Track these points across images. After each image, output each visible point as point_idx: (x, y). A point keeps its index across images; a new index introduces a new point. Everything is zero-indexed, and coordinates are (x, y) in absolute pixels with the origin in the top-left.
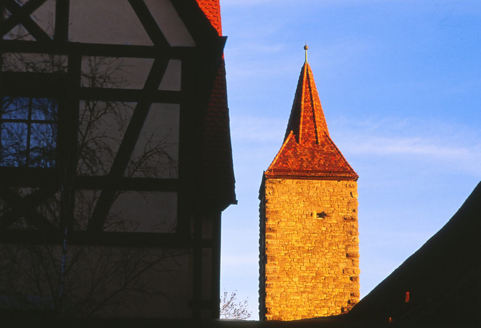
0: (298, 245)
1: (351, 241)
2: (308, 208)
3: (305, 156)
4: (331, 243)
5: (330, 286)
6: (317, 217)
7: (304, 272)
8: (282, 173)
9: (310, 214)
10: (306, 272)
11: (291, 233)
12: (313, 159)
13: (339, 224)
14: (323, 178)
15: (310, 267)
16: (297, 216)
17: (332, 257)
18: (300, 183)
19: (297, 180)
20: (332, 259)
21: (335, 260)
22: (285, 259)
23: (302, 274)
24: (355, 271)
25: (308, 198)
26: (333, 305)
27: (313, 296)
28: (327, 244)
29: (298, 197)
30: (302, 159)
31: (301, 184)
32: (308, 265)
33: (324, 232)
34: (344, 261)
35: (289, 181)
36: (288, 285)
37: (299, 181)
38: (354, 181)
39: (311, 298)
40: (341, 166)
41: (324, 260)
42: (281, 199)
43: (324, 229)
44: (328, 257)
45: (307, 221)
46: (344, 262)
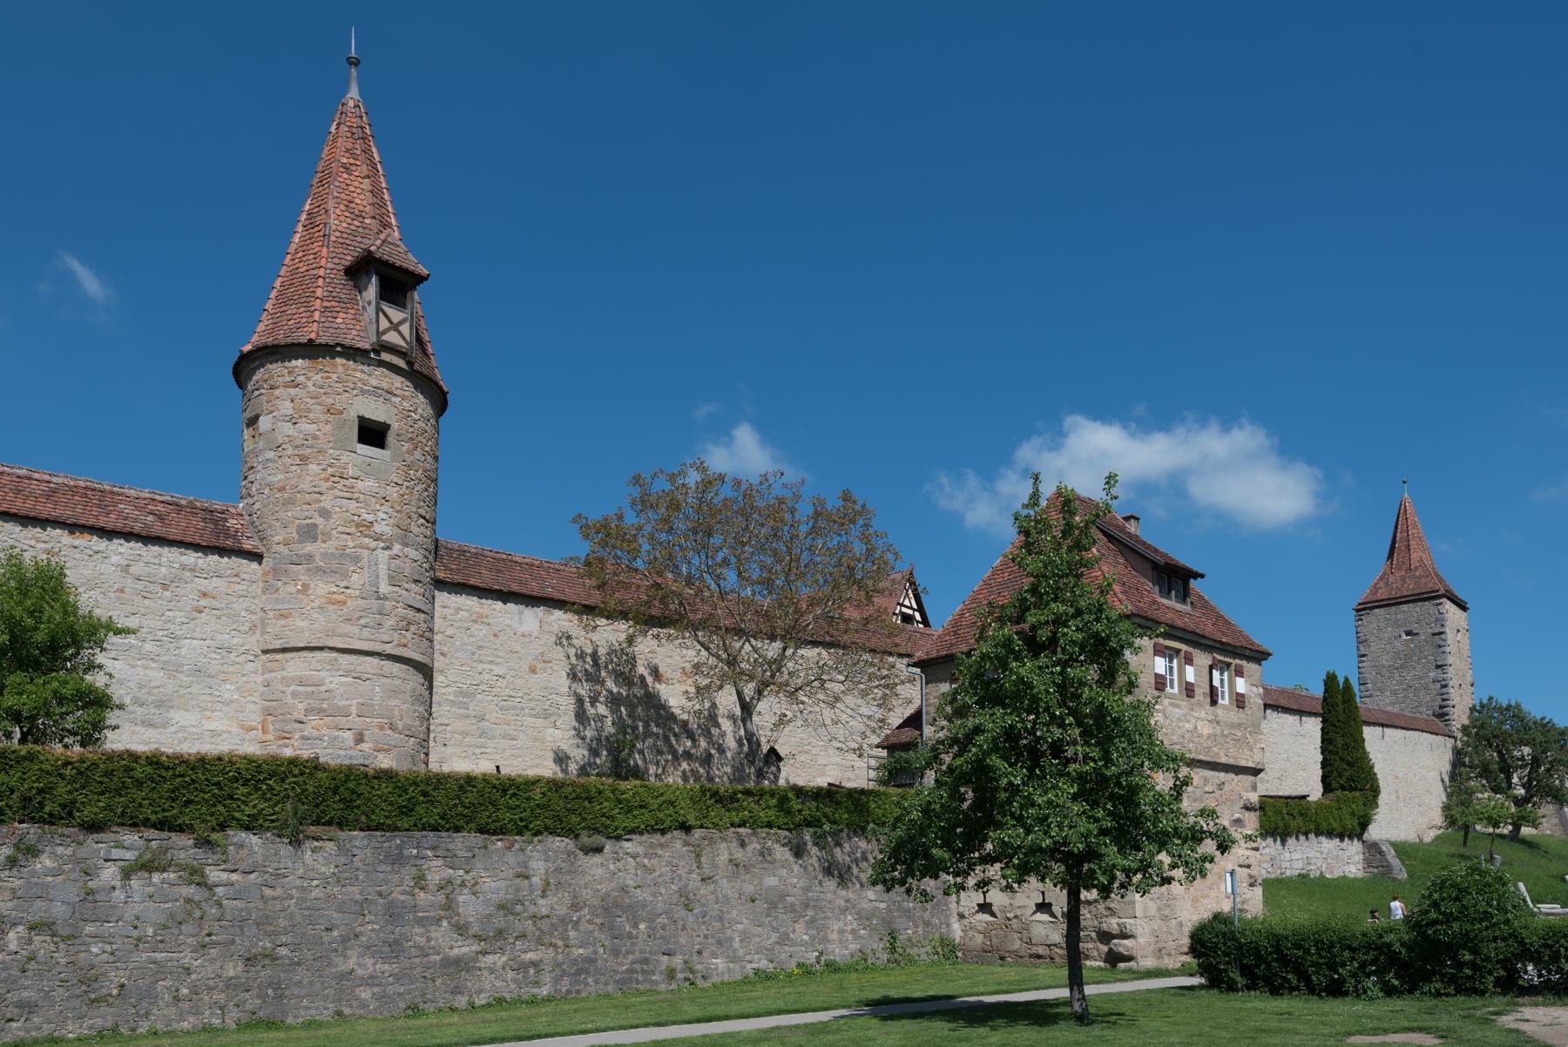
12: (1403, 586)
35: (1377, 611)
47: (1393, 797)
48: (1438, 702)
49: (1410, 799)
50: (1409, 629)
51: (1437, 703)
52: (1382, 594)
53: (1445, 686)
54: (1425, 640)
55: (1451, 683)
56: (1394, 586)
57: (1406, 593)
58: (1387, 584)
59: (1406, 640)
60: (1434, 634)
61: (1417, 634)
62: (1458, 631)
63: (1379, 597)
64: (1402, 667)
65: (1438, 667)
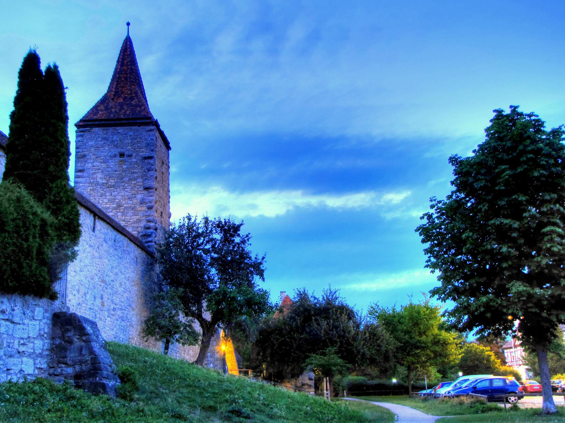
0: (102, 182)
2: (112, 150)
7: (106, 204)
8: (91, 123)
12: (120, 110)
15: (112, 199)
16: (102, 158)
18: (106, 130)
19: (103, 128)
21: (133, 192)
22: (90, 195)
25: (113, 142)
30: (111, 111)
33: (125, 169)
35: (96, 129)
37: (105, 128)
38: (153, 125)
45: (110, 161)
46: (141, 194)
47: (98, 302)
48: (143, 224)
49: (114, 309)
50: (123, 150)
51: (142, 225)
52: (101, 115)
53: (150, 208)
54: (136, 163)
56: (113, 110)
58: (107, 108)
59: (121, 161)
60: (146, 158)
61: (130, 156)
64: (113, 186)
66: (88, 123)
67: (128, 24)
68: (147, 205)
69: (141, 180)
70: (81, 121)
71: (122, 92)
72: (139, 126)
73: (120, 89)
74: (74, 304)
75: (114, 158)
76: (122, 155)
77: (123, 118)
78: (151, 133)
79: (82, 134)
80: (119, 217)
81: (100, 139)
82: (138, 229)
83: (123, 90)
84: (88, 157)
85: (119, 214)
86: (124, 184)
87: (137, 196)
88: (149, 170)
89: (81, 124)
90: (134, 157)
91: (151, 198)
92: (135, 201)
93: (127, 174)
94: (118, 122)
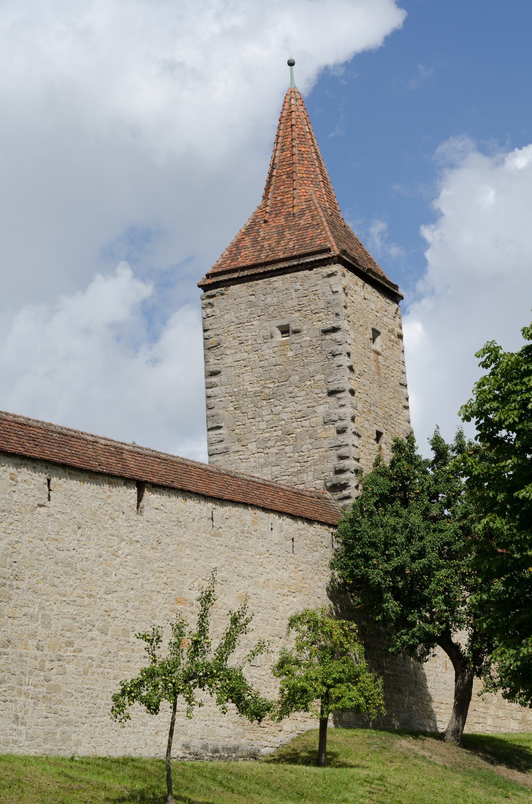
0: (253, 389)
1: (333, 365)
2: (265, 324)
3: (269, 239)
4: (303, 377)
5: (304, 448)
6: (283, 337)
9: (269, 334)
10: (268, 430)
11: (241, 371)
12: (278, 242)
13: (314, 340)
14: (286, 271)
16: (250, 343)
17: (305, 397)
19: (247, 284)
20: (306, 401)
22: (234, 417)
23: (261, 435)
24: (341, 415)
26: (310, 478)
27: (278, 468)
28: (297, 378)
29: (249, 310)
30: (262, 246)
31: (254, 289)
32: (268, 418)
34: (325, 401)
35: (235, 289)
36: (241, 457)
38: (335, 264)
39: (276, 473)
40: (318, 242)
41: (292, 406)
42: (224, 319)
43: (290, 354)
44: (299, 399)
45: (265, 346)
48: (334, 463)
50: (284, 322)
53: (341, 431)
54: (311, 345)
55: (352, 427)
56: (266, 244)
57: (281, 256)
58: (255, 241)
59: (283, 344)
60: (325, 332)
61: (296, 332)
62: (376, 333)
63: (241, 262)
65: (331, 393)
66: (221, 278)
67: (291, 64)
68: (337, 424)
69: (323, 377)
70: (208, 276)
71: (283, 204)
72: (311, 269)
73: (279, 198)
74: (94, 656)
75: (270, 340)
76: (285, 330)
77: (281, 257)
78: (332, 279)
79: (211, 300)
80: (288, 455)
81: (243, 306)
82: (323, 475)
83: (285, 200)
84: (225, 345)
85: (287, 449)
86: (290, 389)
87: (316, 409)
88: (334, 356)
89: (210, 281)
90: (305, 332)
91: (343, 410)
92: (313, 420)
93: (296, 369)
94: (269, 268)
